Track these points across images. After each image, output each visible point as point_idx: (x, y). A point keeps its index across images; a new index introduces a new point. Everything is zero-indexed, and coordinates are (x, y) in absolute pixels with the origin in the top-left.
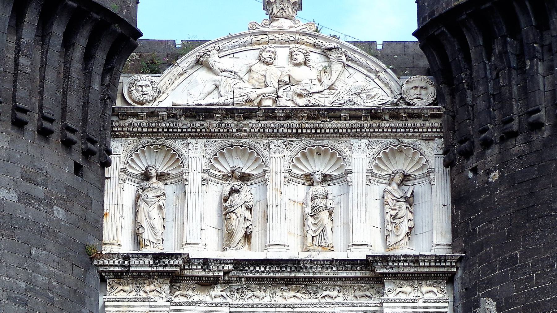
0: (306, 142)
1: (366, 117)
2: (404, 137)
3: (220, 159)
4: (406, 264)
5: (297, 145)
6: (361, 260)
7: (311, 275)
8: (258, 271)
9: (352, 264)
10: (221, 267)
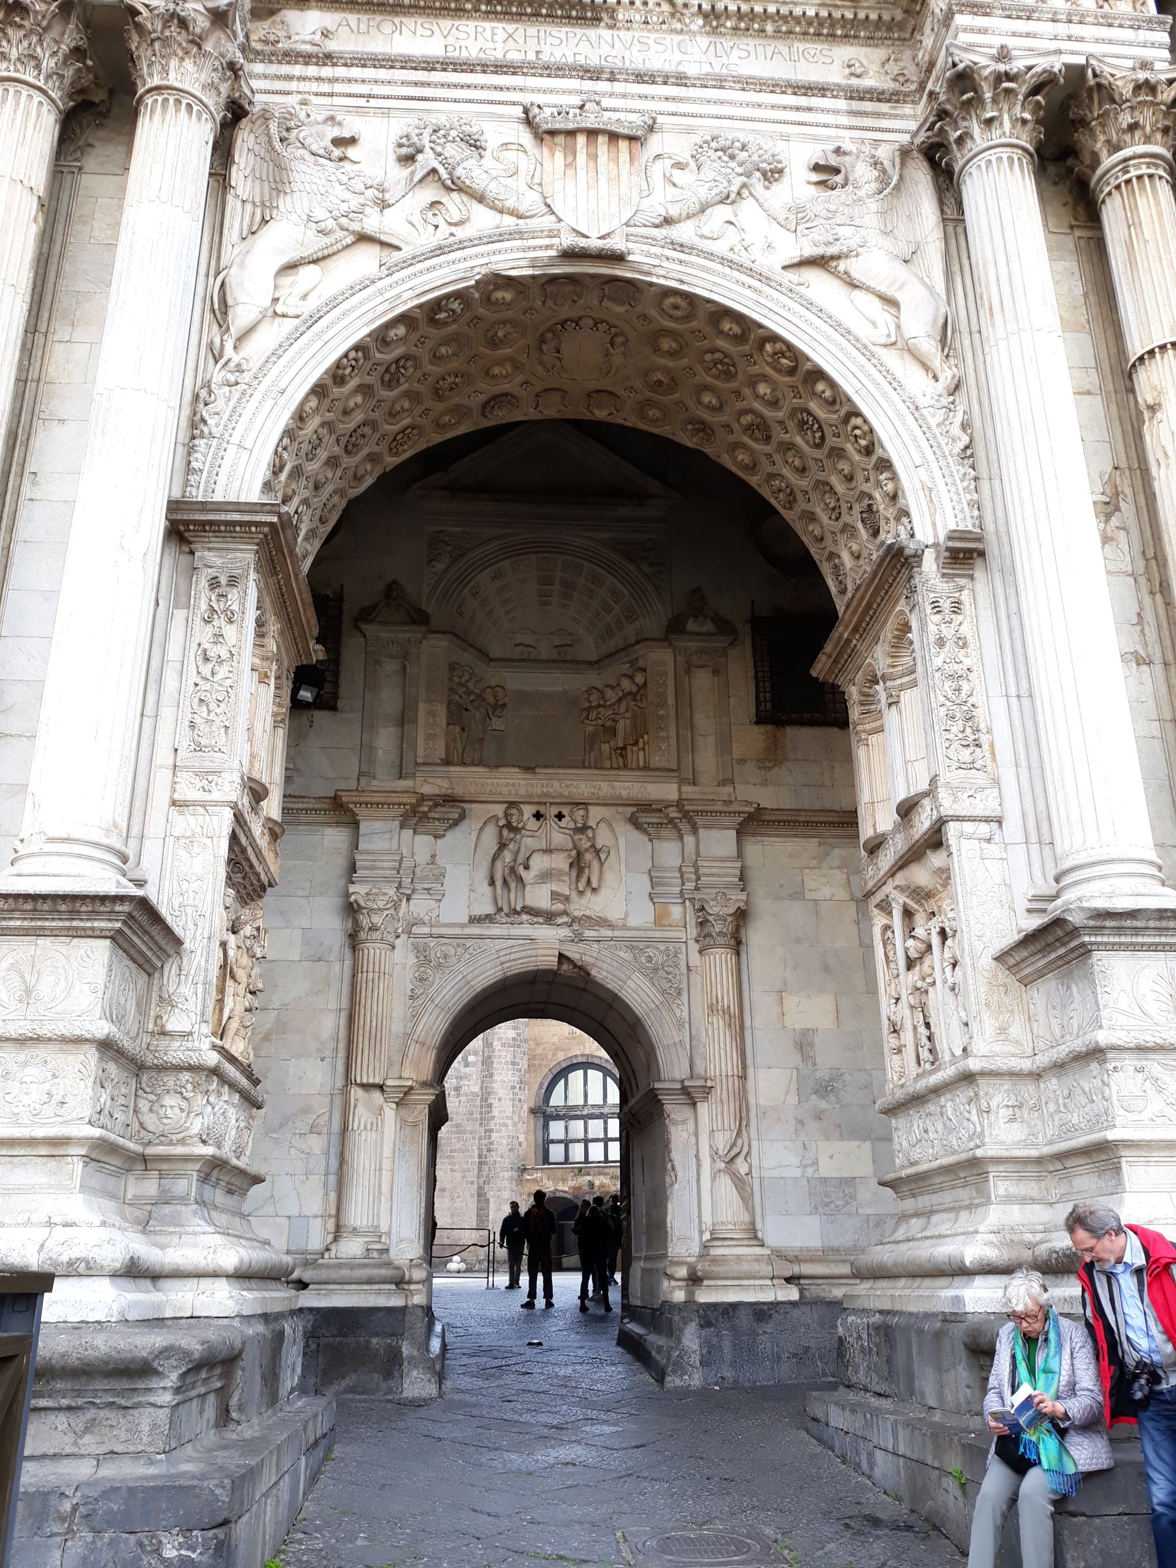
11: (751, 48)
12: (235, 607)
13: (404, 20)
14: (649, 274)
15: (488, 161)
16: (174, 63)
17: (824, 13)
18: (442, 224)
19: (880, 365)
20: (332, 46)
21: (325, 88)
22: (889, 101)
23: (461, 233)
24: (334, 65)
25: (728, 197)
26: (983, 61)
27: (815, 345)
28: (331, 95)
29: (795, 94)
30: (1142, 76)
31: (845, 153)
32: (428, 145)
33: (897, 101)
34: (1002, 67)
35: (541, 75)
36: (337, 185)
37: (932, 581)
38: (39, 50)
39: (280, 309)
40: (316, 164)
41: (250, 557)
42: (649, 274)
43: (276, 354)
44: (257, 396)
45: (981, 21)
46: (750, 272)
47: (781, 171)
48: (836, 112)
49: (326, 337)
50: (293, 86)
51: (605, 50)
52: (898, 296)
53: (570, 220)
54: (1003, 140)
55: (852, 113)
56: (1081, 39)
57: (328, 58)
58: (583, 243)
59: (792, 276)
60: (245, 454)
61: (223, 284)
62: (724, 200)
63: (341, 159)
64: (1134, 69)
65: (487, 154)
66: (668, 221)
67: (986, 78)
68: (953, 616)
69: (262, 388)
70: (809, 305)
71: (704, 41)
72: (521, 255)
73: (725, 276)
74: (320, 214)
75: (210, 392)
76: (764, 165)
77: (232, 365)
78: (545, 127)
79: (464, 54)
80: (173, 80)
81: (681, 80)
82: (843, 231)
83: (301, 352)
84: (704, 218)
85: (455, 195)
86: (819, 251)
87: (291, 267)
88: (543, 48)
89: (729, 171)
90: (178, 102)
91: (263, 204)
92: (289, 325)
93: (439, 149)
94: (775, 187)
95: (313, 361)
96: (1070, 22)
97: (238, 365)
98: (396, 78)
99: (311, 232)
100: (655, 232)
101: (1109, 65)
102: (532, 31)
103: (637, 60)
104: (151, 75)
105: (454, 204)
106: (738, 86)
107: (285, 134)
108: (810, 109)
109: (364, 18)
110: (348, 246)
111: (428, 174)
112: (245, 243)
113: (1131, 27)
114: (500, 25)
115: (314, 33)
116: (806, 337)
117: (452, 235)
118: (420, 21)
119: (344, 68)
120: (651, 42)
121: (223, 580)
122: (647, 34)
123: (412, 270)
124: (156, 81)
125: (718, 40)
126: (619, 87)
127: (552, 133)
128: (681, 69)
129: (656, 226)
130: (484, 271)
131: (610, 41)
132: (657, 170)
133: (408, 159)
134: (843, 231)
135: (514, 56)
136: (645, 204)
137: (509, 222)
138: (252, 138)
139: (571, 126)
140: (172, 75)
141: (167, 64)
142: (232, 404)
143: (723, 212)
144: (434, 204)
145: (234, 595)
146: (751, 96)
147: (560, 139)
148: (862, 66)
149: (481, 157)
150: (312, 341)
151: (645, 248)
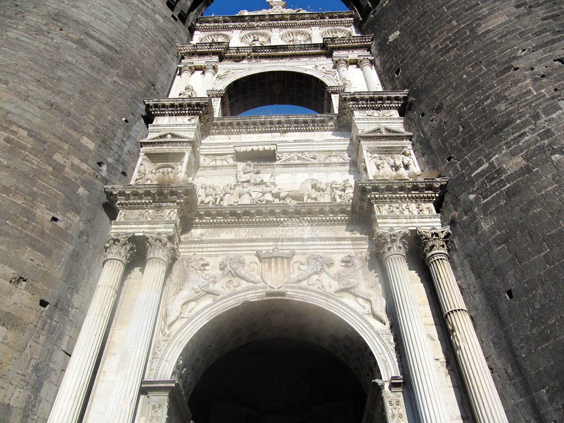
0: (289, 30)
1: (317, 17)
2: (336, 26)
3: (248, 37)
4: (344, 42)
5: (284, 31)
6: (320, 44)
7: (294, 52)
8: (265, 52)
9: (316, 46)
10: (246, 51)
11: (323, 229)
12: (159, 415)
13: (224, 229)
14: (294, 298)
16: (157, 251)
17: (343, 218)
18: (232, 286)
19: (366, 321)
20: (204, 238)
21: (201, 250)
23: (238, 289)
25: (317, 272)
26: (386, 231)
27: (345, 316)
28: (202, 252)
29: (336, 241)
30: (433, 231)
31: (351, 257)
34: (391, 233)
36: (201, 278)
37: (389, 394)
39: (182, 316)
40: (196, 272)
41: (167, 398)
42: (294, 298)
43: (180, 331)
44: (173, 344)
45: (385, 221)
46: (324, 295)
47: (333, 264)
48: (348, 245)
49: (195, 324)
50: (192, 250)
51: (280, 233)
52: (371, 298)
53: (269, 283)
54: (394, 253)
55: (353, 245)
56: (414, 223)
58: (273, 290)
59: (337, 295)
60: (168, 363)
61: (166, 309)
62: (316, 273)
63: (204, 270)
64: (431, 230)
65: (246, 265)
66: (299, 281)
68: (397, 406)
69: (175, 341)
70: (343, 303)
71: (309, 228)
72: (255, 295)
73: (316, 297)
74: (196, 287)
75: (159, 344)
76: (327, 262)
77: (166, 334)
78: (262, 257)
79: (241, 238)
81: (302, 240)
82: (351, 280)
83: (187, 330)
84: (310, 279)
85: (236, 278)
86: (345, 287)
87: (186, 303)
88: (264, 234)
90: (157, 261)
91: (180, 284)
92: (185, 320)
93: (231, 265)
94: (331, 268)
95: (191, 332)
96: (411, 218)
97: (168, 334)
99: (193, 293)
100: (295, 285)
101: (423, 229)
102: (260, 229)
103: (289, 235)
104: (150, 255)
105: (236, 280)
108: (341, 245)
109: (213, 229)
110: (204, 295)
111: (228, 272)
112: (174, 296)
113: (429, 218)
114: (251, 229)
116: (342, 314)
117: (234, 290)
118: (228, 229)
120: (294, 229)
121: (157, 406)
123: (222, 302)
124: (151, 256)
125: (313, 227)
126: (284, 243)
127: (265, 258)
128: (303, 237)
129: (295, 283)
130: (244, 300)
132: (296, 266)
133: (222, 269)
134: (351, 280)
135: (254, 237)
136: (292, 277)
137: (251, 284)
138: (178, 266)
139: (270, 256)
140: (156, 254)
142: (165, 347)
143: (316, 277)
144: (229, 281)
145: (159, 411)
146: (323, 242)
147: (267, 260)
150: (191, 325)
151: (292, 290)
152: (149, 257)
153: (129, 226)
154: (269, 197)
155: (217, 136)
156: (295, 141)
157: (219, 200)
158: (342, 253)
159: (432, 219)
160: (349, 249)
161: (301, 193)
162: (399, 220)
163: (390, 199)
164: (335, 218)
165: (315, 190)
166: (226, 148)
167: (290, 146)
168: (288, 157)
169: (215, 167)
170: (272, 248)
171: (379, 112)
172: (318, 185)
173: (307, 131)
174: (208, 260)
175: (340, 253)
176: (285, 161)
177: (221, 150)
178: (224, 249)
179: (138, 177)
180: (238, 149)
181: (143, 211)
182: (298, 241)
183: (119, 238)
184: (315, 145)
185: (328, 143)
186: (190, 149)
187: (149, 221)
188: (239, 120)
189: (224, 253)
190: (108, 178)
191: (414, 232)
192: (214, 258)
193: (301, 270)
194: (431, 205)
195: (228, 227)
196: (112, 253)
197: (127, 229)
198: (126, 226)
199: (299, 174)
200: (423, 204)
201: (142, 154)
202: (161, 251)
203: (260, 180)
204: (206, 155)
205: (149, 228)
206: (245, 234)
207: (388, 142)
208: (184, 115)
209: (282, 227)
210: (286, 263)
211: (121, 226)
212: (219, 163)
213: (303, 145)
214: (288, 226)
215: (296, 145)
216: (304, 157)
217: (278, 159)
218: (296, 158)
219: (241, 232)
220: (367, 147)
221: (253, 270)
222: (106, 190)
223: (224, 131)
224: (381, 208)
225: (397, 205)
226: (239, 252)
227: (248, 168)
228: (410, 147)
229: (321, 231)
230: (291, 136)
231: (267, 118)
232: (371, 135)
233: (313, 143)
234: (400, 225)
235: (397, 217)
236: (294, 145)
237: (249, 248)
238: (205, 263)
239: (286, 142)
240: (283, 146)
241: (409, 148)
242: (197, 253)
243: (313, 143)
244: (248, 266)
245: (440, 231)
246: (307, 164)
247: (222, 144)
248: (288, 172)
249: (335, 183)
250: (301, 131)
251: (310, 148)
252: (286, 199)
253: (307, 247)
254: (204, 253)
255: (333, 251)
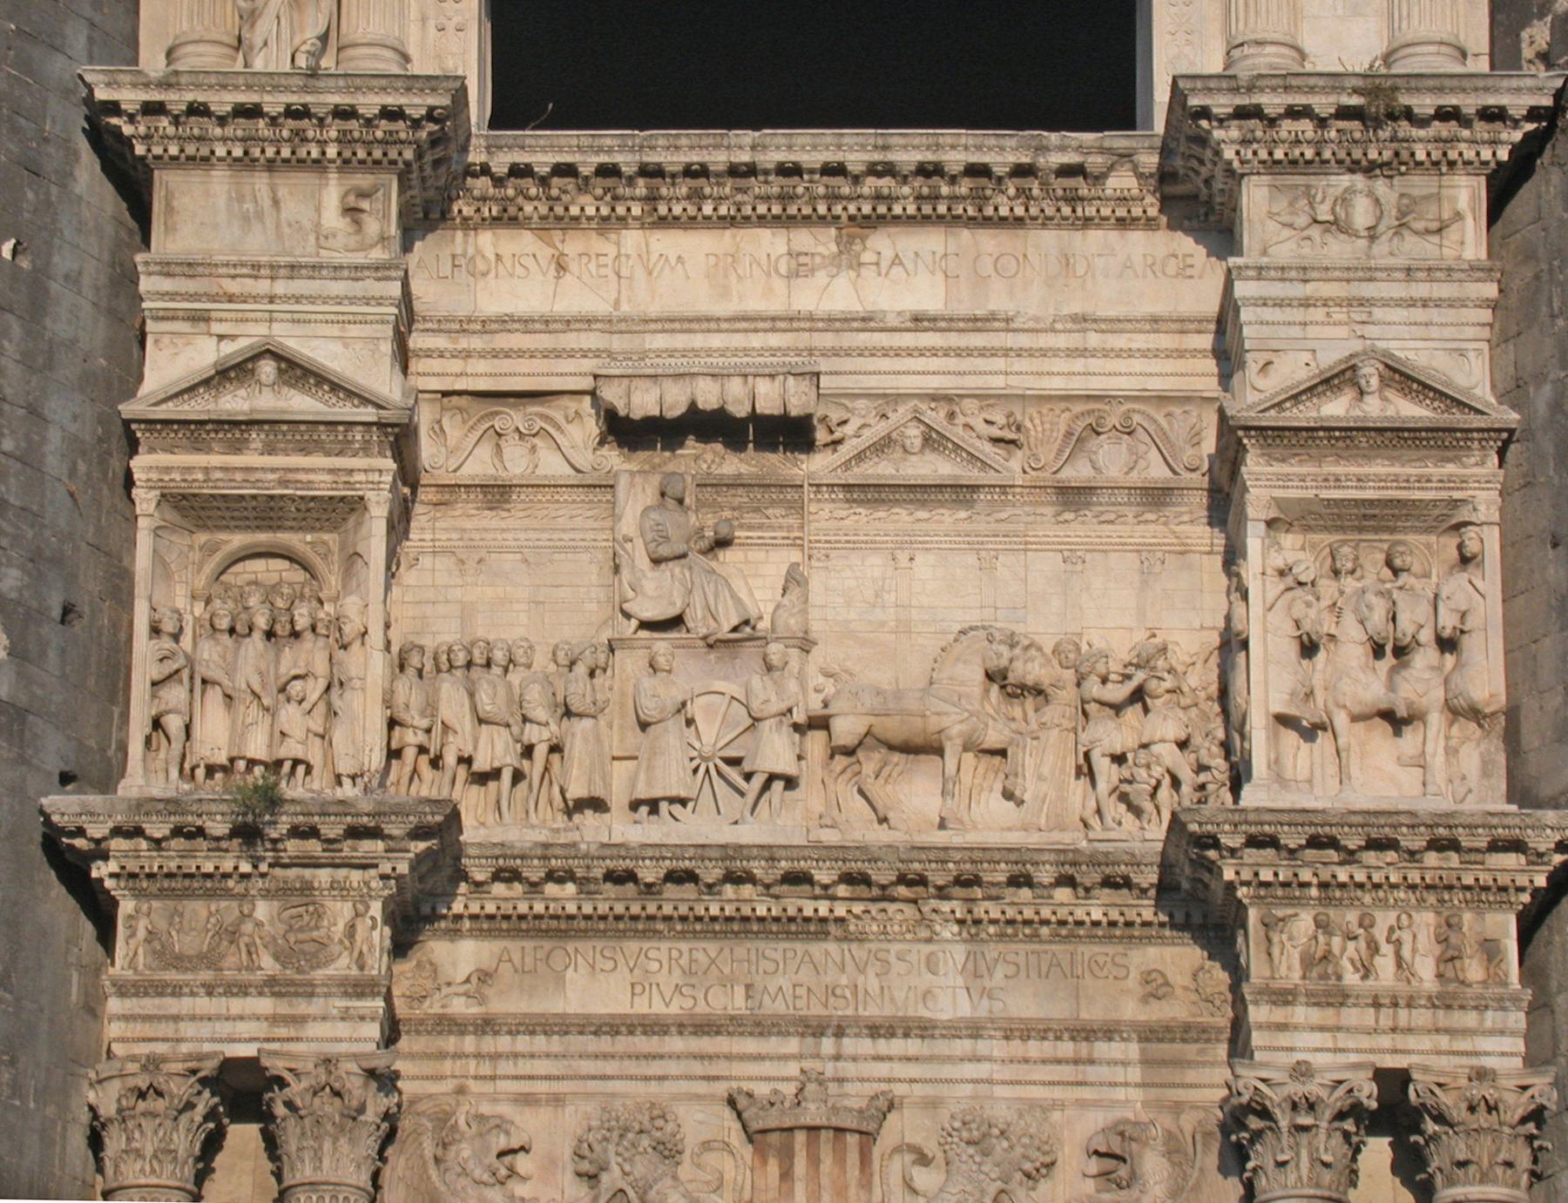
11: (1021, 959)
13: (580, 945)
15: (685, 1170)
16: (327, 1145)
17: (1114, 915)
21: (486, 1068)
22: (1196, 1041)
24: (496, 1033)
28: (493, 1078)
29: (1073, 1039)
30: (1478, 1091)
32: (614, 1160)
33: (1208, 1041)
35: (751, 1034)
38: (175, 1136)
45: (1279, 1014)
50: (447, 1066)
55: (1147, 1062)
57: (487, 1025)
65: (686, 1156)
67: (1279, 1105)
71: (959, 952)
76: (1028, 1166)
80: (327, 1171)
81: (925, 1029)
88: (758, 980)
89: (982, 1176)
93: (627, 1168)
94: (1044, 1186)
98: (572, 1049)
106: (999, 1034)
107: (440, 1152)
109: (529, 944)
113: (1476, 1008)
115: (468, 981)
118: (599, 944)
119: (508, 1038)
120: (893, 960)
122: (885, 946)
126: (849, 1045)
127: (764, 1131)
131: (838, 960)
132: (896, 1165)
133: (592, 1178)
139: (788, 1123)
140: (326, 1163)
141: (321, 1147)
147: (774, 1138)
148: (1167, 984)
149: (678, 1164)
152: (299, 1178)
153: (185, 1005)
154: (776, 751)
155: (486, 240)
156: (920, 321)
157: (540, 752)
158: (1096, 1104)
159: (1490, 1014)
160: (1126, 1084)
161: (934, 723)
162: (1351, 1016)
163: (1323, 886)
164: (1080, 914)
165: (1003, 687)
166: (546, 354)
167: (886, 352)
168: (879, 429)
169: (497, 493)
170: (793, 1069)
171: (1380, 186)
172: (1018, 666)
173: (986, 222)
174: (529, 1124)
175: (1082, 1104)
176: (860, 457)
177: (524, 365)
178: (587, 1067)
179: (156, 672)
180: (612, 394)
181: (229, 909)
182: (906, 1035)
183: (160, 1082)
184: (1020, 353)
185: (1094, 340)
186: (388, 478)
187: (271, 982)
188: (610, 151)
189: (592, 1085)
190: (23, 699)
191: (1393, 1081)
192: (545, 1113)
193: (915, 1191)
194: (1505, 926)
195: (603, 934)
196: (139, 1154)
197: (176, 1018)
198: (172, 1005)
199: (931, 558)
200: (1467, 917)
201: (145, 500)
202: (343, 1142)
203: (735, 621)
204: (445, 394)
205: (274, 1019)
206: (677, 976)
207: (1379, 468)
208: (319, 165)
209: (838, 939)
210: (853, 1157)
211: (149, 1005)
212: (516, 463)
213: (959, 352)
214: (861, 938)
215: (921, 352)
216: (957, 433)
217: (821, 436)
218: (918, 442)
219: (655, 966)
220: (1278, 502)
221: (718, 1188)
222: (55, 818)
223: (528, 208)
224: (1275, 938)
225: (1352, 916)
226: (653, 1087)
227: (674, 522)
228: (1486, 504)
229: (1011, 970)
230: (897, 260)
231: (765, 147)
232: (1302, 415)
233: (1010, 340)
234: (1344, 1040)
235: (1339, 998)
236: (910, 352)
237: (698, 1068)
238: (515, 1144)
239: (867, 322)
240: (848, 353)
241: (1481, 516)
242: (471, 1083)
243: (1010, 340)
244: (699, 1166)
245: (1512, 1083)
246: (974, 488)
247: (526, 323)
248: (872, 546)
249: (1101, 668)
250: (952, 221)
251: (994, 376)
252: (860, 754)
253: (948, 1071)
254: (504, 1086)
255: (1058, 1093)
